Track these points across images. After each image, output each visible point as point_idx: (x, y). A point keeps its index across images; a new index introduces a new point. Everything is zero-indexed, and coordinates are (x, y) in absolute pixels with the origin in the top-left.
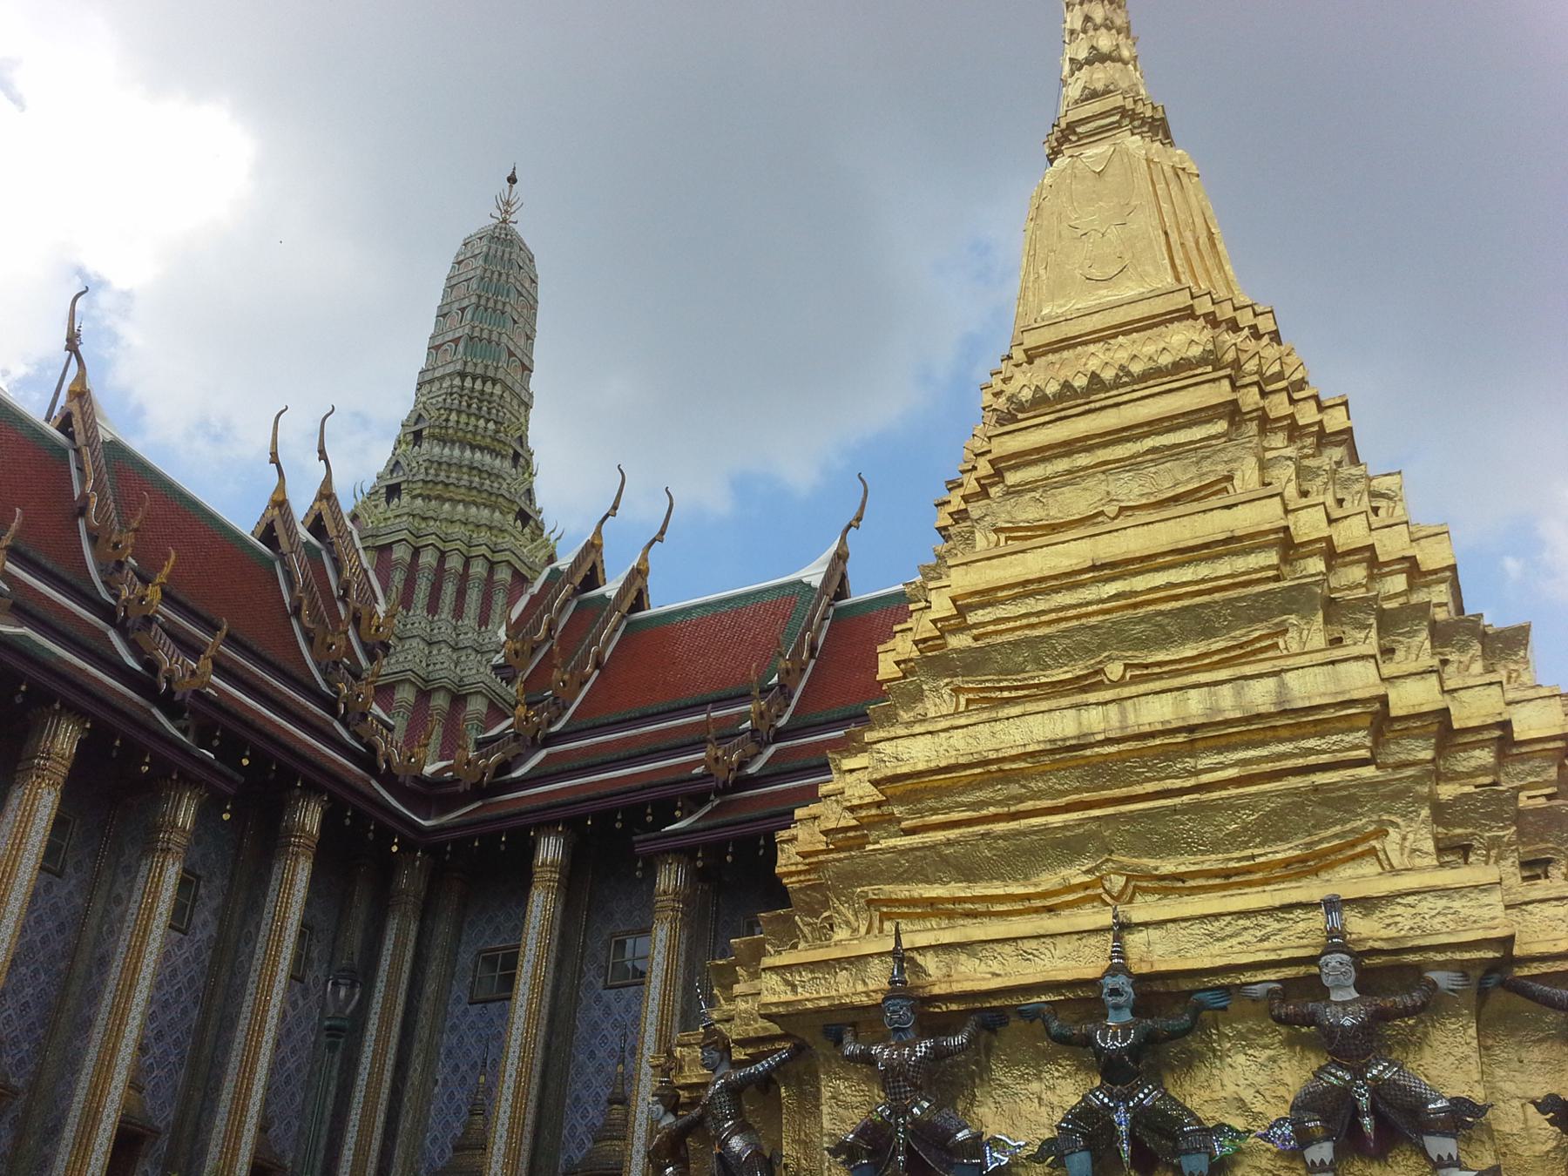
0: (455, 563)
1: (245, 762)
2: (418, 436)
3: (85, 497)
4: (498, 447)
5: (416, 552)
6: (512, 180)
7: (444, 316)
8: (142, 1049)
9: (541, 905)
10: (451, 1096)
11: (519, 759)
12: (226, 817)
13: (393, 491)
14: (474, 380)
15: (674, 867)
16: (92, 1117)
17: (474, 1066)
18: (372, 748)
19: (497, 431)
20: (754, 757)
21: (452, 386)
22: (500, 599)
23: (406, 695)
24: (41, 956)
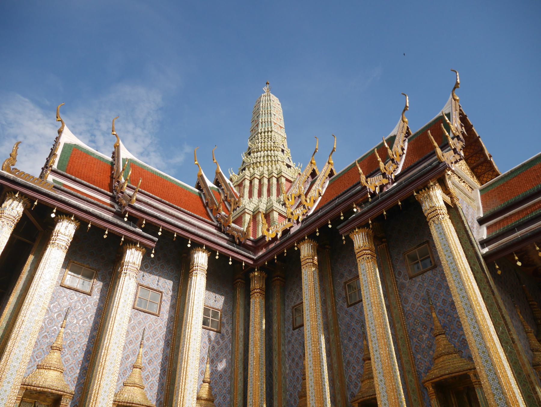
9: (309, 275)
17: (300, 357)
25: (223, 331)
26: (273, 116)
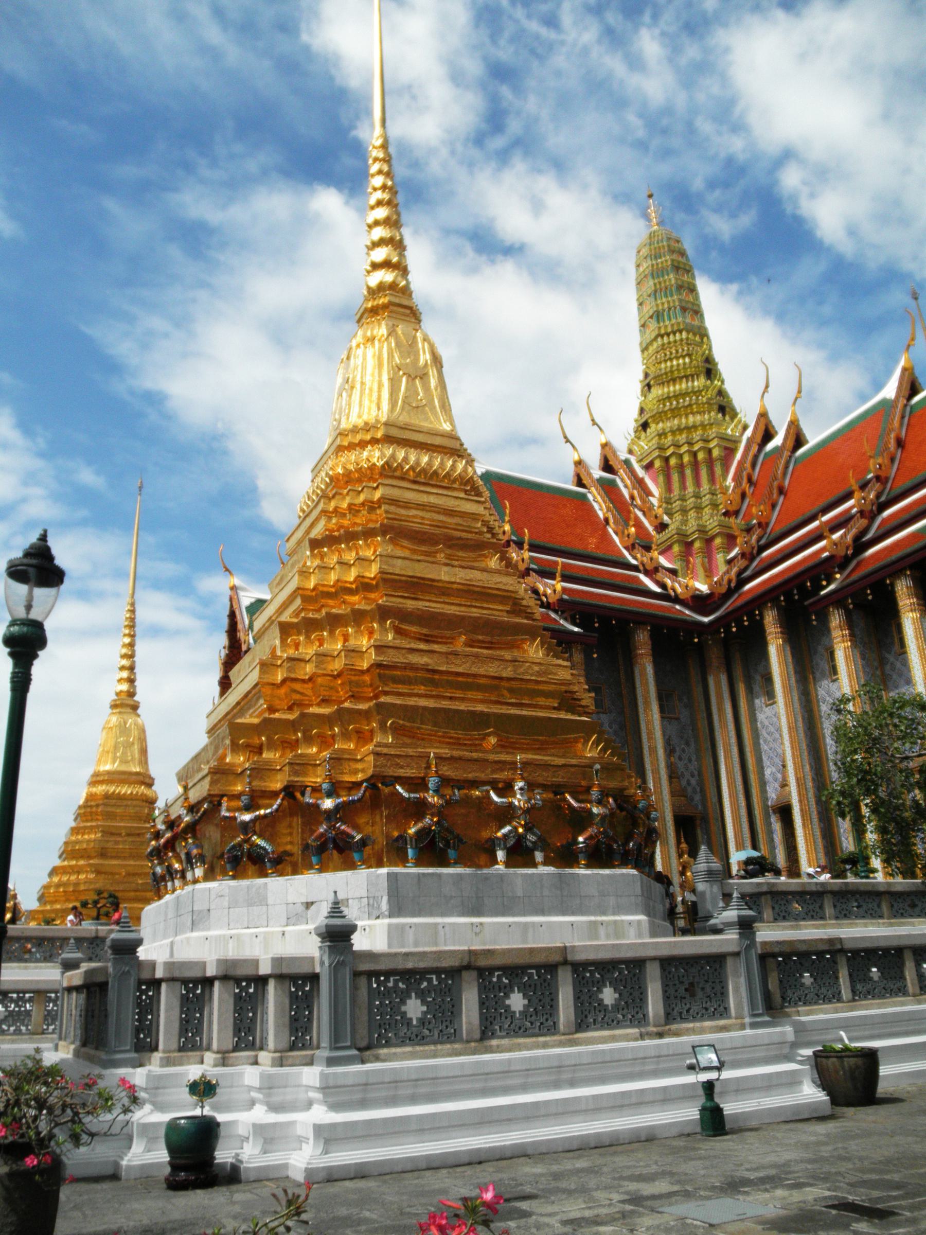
1: (597, 625)
2: (649, 386)
5: (667, 460)
12: (595, 656)
13: (645, 426)
14: (668, 335)
15: (836, 612)
19: (691, 362)
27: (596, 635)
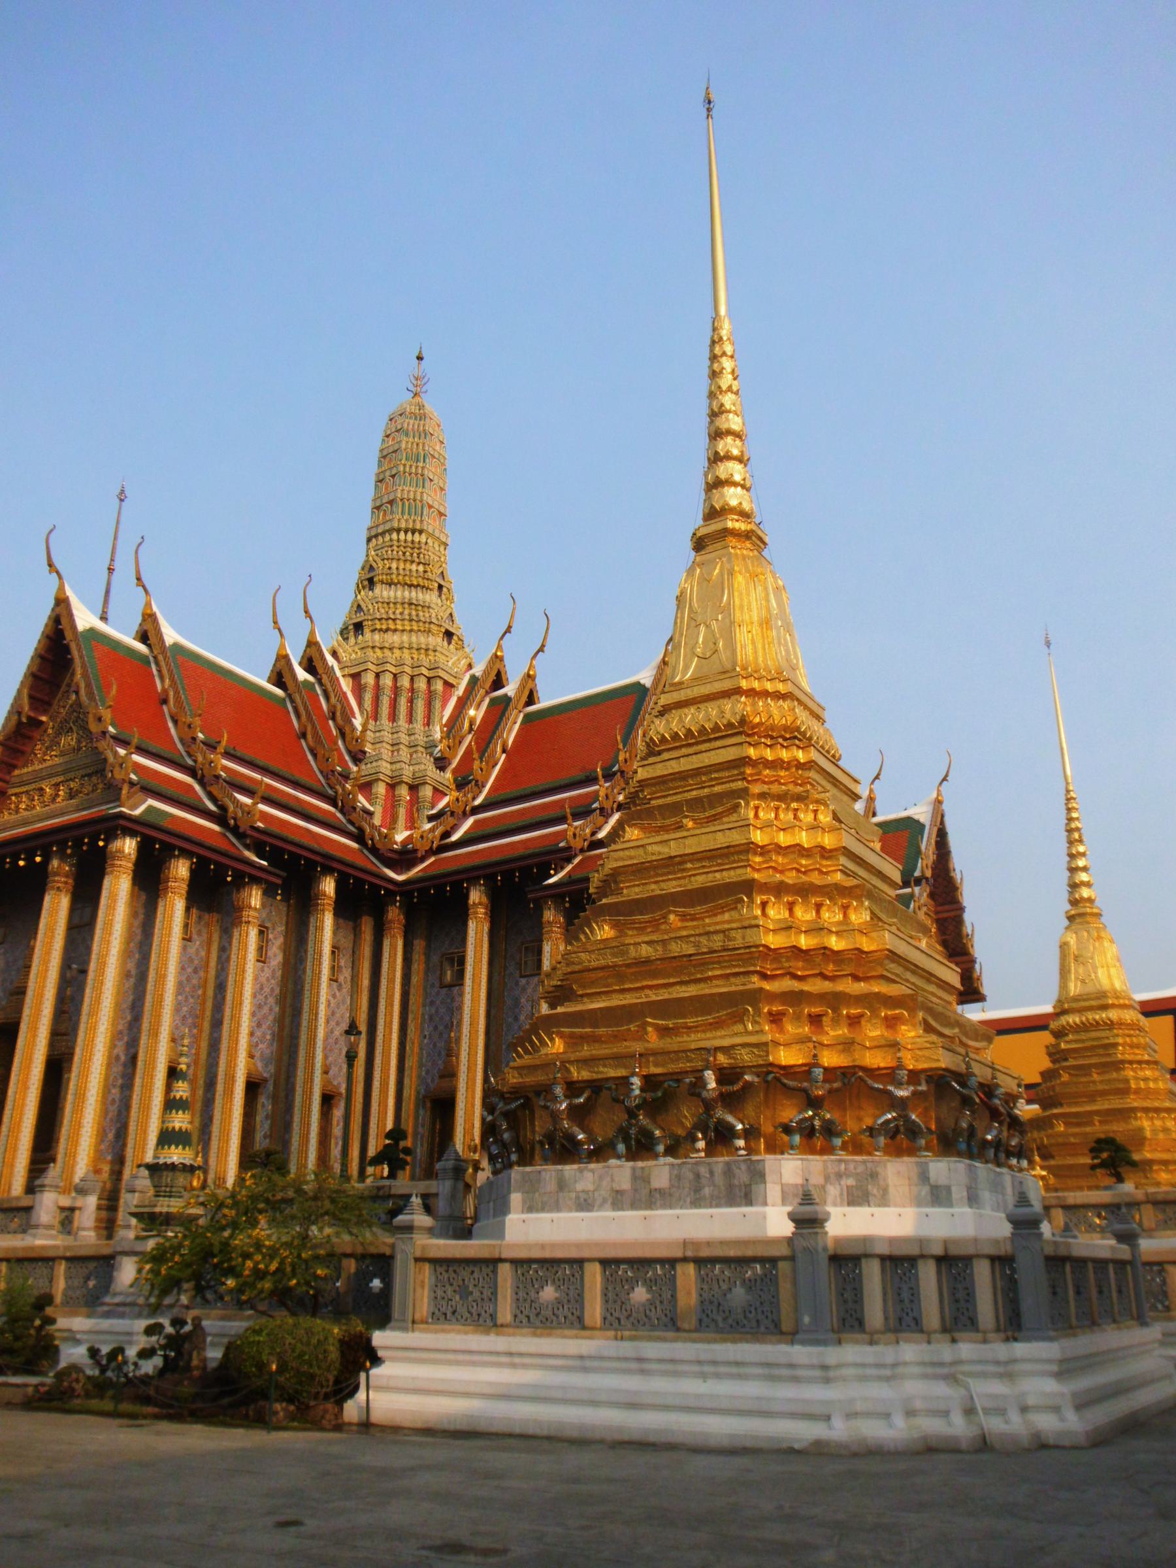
0: (405, 682)
3: (165, 691)
4: (426, 583)
6: (420, 358)
7: (380, 481)
8: (252, 1034)
9: (477, 932)
10: (435, 1045)
11: (454, 828)
14: (406, 532)
16: (231, 1079)
17: (446, 1027)
18: (361, 830)
19: (425, 572)
20: (600, 828)
21: (391, 540)
22: (437, 704)
23: (381, 789)
24: (187, 989)
25: (341, 979)
26: (427, 483)
27: (284, 874)
